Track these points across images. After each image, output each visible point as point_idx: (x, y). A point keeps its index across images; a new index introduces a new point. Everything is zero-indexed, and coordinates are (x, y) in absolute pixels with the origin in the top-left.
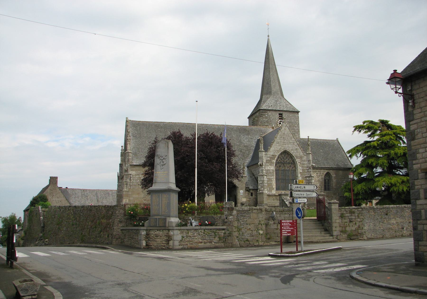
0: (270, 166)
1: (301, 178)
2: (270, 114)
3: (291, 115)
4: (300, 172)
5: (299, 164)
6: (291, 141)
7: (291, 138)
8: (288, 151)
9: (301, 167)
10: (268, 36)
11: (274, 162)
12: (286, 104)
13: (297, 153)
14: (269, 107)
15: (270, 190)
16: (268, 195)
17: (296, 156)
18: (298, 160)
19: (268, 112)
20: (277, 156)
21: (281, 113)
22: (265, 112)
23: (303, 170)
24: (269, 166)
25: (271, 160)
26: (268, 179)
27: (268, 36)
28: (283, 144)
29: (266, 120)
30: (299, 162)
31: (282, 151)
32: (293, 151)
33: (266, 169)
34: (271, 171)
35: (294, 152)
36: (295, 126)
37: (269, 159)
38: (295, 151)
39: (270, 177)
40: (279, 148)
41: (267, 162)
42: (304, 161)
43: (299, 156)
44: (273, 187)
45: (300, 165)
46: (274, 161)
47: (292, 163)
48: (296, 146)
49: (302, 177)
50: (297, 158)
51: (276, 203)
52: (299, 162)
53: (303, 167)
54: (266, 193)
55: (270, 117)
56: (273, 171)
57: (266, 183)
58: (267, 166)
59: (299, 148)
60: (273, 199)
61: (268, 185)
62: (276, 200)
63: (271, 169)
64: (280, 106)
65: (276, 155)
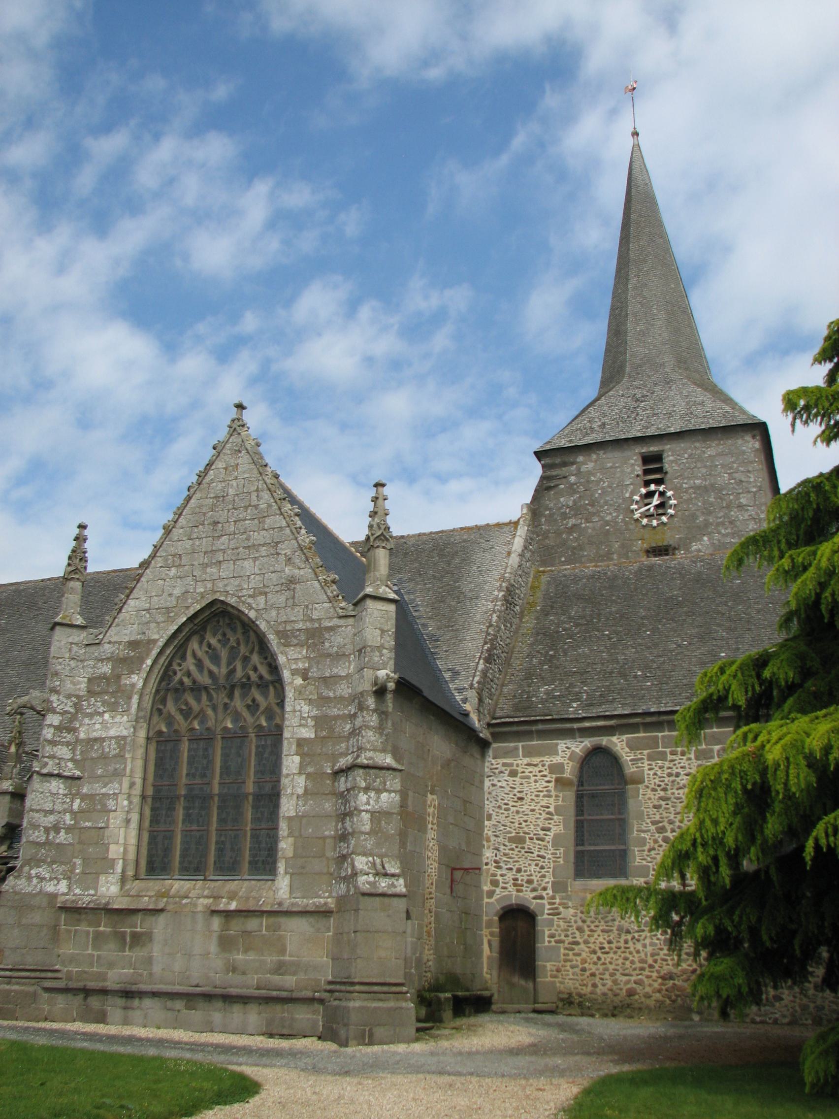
0: (107, 716)
1: (301, 781)
2: (590, 465)
3: (710, 452)
4: (301, 743)
5: (299, 681)
6: (258, 537)
7: (261, 519)
8: (232, 601)
9: (310, 702)
10: (635, 134)
11: (133, 685)
12: (688, 403)
13: (294, 605)
14: (587, 434)
15: (90, 877)
16: (63, 909)
17: (278, 633)
18: (293, 653)
19: (580, 459)
20: (161, 643)
21: (654, 448)
22: (565, 464)
23: (320, 722)
24: (101, 714)
25: (118, 677)
26: (83, 798)
27: (635, 134)
28: (204, 566)
29: (571, 503)
30: (294, 673)
31: (191, 612)
32: (261, 599)
33: (82, 736)
34: (111, 748)
35: (273, 606)
36: (741, 507)
37: (106, 669)
38: (281, 599)
39: (98, 788)
40: (177, 592)
41: (91, 693)
42: (339, 656)
43: (300, 625)
44: (111, 856)
45: (299, 692)
46: (135, 678)
47: (263, 685)
48: (289, 560)
49: (308, 776)
50: (287, 645)
51: (111, 965)
52: (294, 673)
53: (323, 700)
54: (53, 896)
55: (588, 481)
56: (122, 748)
57: (56, 828)
58: (91, 716)
59: (307, 572)
60: (99, 939)
61: (80, 842)
62: (112, 945)
63: (113, 733)
64: (654, 415)
65: (155, 641)
